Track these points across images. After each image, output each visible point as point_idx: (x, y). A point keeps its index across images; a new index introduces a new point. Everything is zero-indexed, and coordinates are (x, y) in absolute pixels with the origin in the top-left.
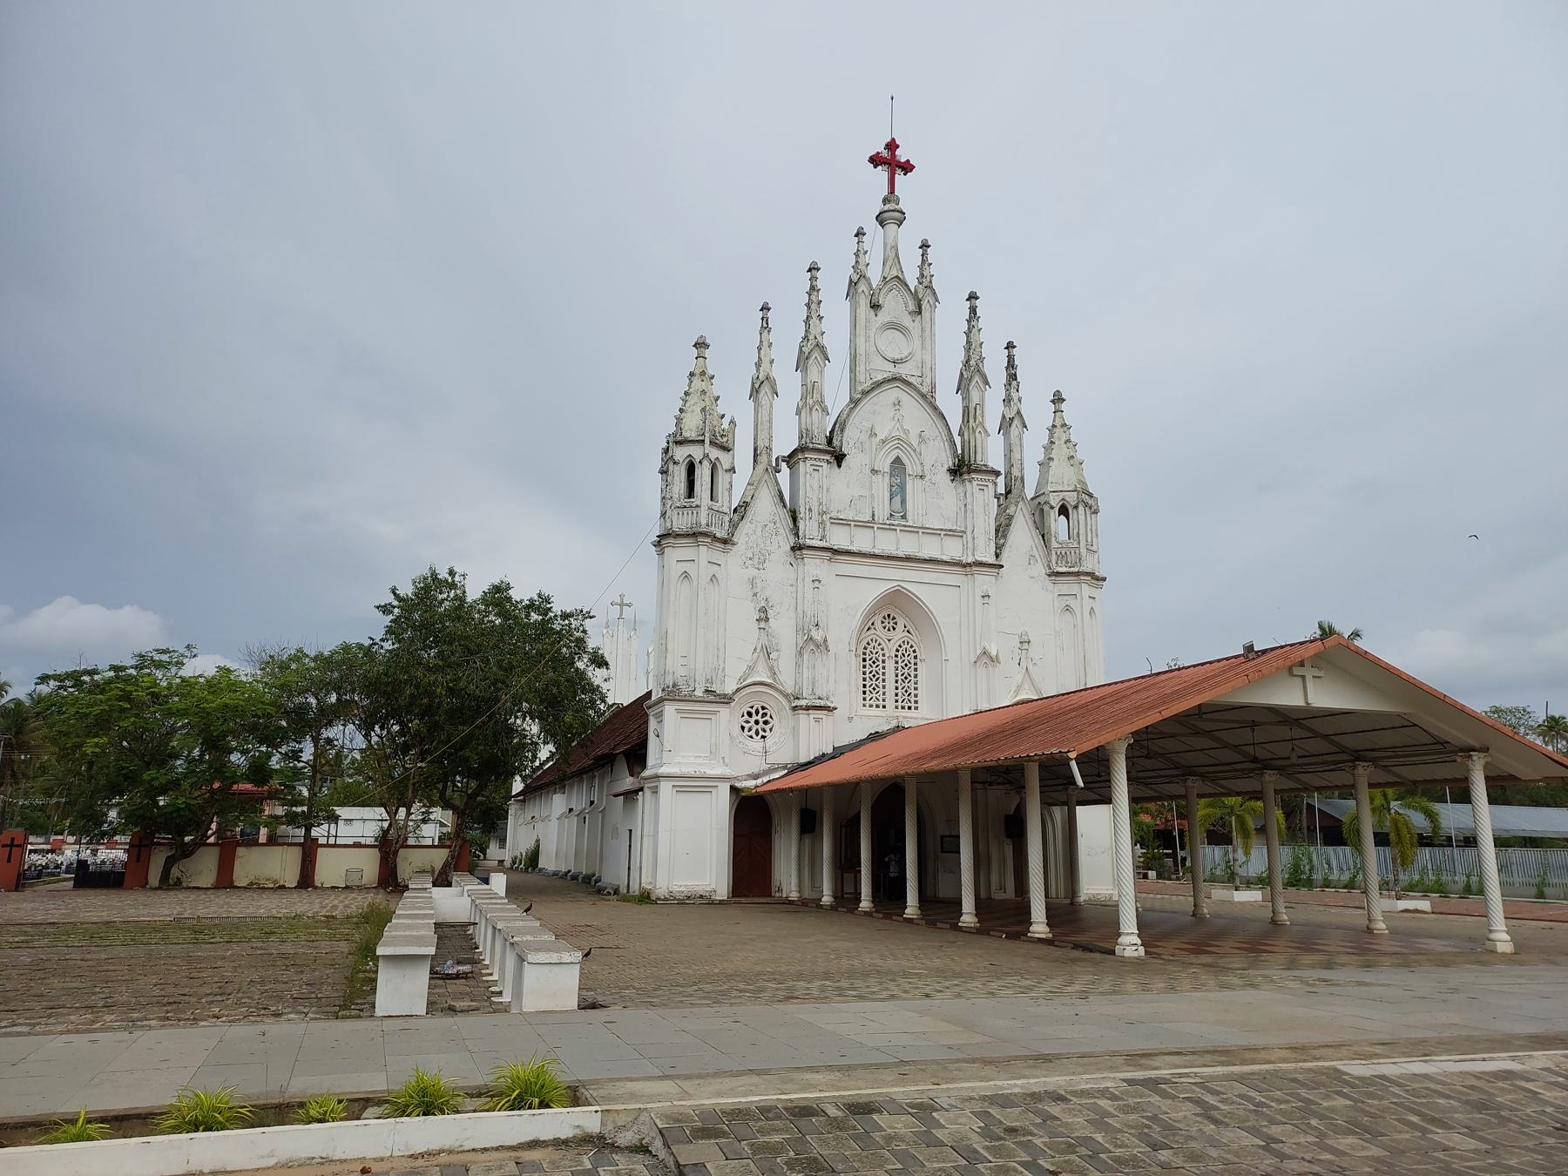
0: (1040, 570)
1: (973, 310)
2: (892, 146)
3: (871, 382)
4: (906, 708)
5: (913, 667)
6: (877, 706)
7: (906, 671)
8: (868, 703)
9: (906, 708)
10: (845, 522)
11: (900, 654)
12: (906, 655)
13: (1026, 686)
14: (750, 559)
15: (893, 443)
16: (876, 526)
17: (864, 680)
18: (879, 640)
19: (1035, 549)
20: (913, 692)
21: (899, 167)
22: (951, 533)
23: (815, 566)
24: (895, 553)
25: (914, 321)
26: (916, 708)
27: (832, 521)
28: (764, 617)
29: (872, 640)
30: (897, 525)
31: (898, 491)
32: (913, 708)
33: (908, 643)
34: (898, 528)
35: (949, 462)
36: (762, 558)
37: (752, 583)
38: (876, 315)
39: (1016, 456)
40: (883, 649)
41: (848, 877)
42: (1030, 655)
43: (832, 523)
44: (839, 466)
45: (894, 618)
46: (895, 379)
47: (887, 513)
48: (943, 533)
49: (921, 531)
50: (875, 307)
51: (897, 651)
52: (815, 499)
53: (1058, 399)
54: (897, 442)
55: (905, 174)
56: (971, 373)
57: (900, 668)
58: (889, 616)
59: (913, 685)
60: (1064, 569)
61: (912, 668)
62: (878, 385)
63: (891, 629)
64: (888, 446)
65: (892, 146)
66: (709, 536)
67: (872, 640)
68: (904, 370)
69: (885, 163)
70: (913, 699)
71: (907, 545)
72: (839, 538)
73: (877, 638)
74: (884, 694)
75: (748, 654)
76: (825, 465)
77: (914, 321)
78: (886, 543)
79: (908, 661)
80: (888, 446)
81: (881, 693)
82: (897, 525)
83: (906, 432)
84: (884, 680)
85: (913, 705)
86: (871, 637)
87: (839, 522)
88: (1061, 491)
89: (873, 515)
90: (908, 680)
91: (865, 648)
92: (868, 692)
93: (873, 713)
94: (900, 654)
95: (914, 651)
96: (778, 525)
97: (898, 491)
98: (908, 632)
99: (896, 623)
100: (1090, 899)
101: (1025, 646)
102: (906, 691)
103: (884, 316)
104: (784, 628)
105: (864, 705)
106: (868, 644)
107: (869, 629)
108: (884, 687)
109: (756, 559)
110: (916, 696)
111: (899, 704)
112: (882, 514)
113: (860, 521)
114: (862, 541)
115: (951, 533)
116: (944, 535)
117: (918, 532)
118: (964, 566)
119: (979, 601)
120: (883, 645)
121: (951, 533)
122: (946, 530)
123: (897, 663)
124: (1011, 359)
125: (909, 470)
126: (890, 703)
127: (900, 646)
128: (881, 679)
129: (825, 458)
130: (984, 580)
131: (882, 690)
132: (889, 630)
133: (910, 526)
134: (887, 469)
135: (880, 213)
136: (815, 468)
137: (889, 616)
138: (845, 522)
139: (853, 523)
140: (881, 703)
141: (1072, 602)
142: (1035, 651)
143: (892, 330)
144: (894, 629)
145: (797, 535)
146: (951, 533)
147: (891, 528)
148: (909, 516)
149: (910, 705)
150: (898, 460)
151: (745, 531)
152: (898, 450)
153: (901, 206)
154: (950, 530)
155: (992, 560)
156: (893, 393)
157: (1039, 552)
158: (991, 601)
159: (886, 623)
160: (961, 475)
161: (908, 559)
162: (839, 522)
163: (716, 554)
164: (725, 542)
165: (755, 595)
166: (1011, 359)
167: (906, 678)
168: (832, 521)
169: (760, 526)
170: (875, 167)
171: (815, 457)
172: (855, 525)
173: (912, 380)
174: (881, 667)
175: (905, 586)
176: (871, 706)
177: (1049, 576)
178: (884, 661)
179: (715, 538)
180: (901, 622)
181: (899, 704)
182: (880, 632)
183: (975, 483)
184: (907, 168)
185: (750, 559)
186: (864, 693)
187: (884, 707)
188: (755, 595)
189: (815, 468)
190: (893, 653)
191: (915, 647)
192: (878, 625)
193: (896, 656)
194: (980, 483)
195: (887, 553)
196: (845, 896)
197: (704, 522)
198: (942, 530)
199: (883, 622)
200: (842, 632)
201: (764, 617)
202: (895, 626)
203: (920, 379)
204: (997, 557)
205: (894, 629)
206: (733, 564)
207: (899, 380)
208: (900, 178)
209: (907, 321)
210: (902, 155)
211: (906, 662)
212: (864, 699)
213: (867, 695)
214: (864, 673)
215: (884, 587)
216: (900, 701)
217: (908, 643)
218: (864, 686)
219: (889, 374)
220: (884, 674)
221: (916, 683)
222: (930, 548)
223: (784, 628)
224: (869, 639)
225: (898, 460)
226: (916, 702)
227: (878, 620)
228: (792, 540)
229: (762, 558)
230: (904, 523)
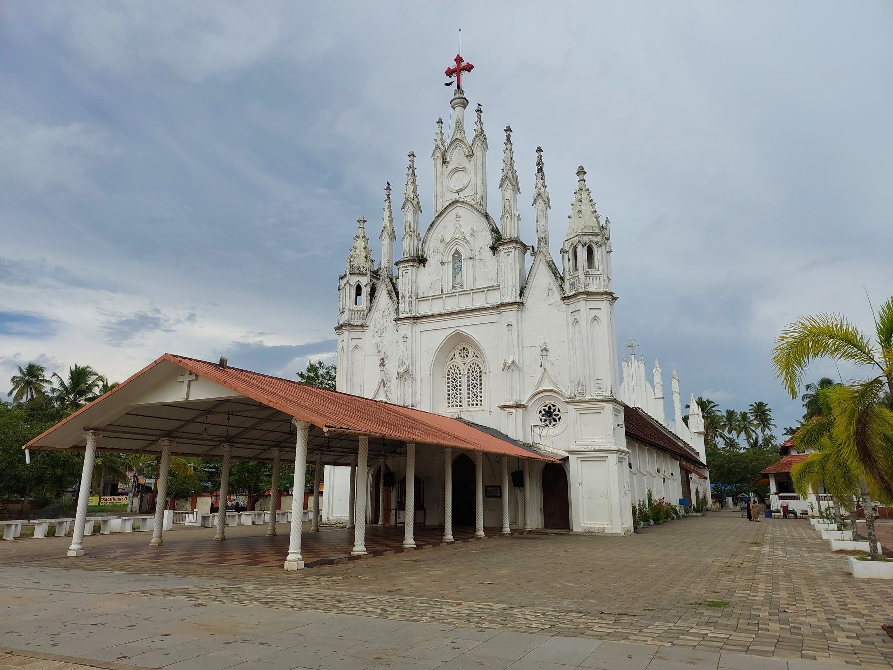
0: (557, 296)
1: (508, 138)
2: (459, 59)
3: (443, 209)
4: (475, 405)
5: (470, 379)
6: (457, 406)
7: (475, 382)
8: (451, 405)
9: (475, 405)
10: (426, 298)
11: (478, 371)
12: (474, 371)
13: (546, 381)
14: (376, 332)
15: (453, 242)
16: (444, 296)
17: (449, 391)
18: (458, 365)
19: (552, 284)
20: (479, 394)
21: (463, 70)
22: (491, 289)
23: (406, 329)
24: (454, 310)
25: (470, 161)
26: (481, 405)
27: (419, 300)
28: (382, 363)
29: (453, 366)
30: (456, 292)
31: (457, 270)
32: (479, 405)
33: (476, 363)
34: (457, 294)
35: (489, 241)
36: (382, 330)
37: (377, 345)
38: (447, 168)
39: (542, 223)
40: (460, 371)
41: (420, 513)
42: (549, 358)
43: (419, 301)
44: (424, 266)
45: (468, 350)
46: (454, 203)
47: (450, 286)
48: (486, 290)
49: (471, 292)
50: (444, 162)
51: (469, 369)
52: (407, 290)
53: (581, 172)
54: (456, 240)
55: (470, 72)
56: (510, 179)
57: (471, 380)
58: (464, 349)
59: (479, 390)
60: (573, 293)
61: (479, 380)
62: (446, 208)
63: (465, 356)
64: (450, 246)
65: (459, 59)
66: (348, 325)
67: (453, 366)
68: (462, 196)
69: (456, 72)
70: (479, 399)
71: (465, 303)
72: (424, 309)
73: (476, 362)
74: (461, 398)
75: (375, 387)
76: (410, 268)
77: (470, 161)
78: (452, 305)
79: (477, 376)
80: (450, 246)
81: (459, 398)
82: (456, 292)
83: (462, 233)
84: (461, 390)
85: (479, 403)
86: (472, 362)
87: (424, 299)
88: (570, 239)
89: (442, 290)
90: (476, 387)
91: (449, 371)
92: (451, 398)
93: (480, 409)
94: (470, 371)
95: (480, 368)
96: (390, 309)
97: (457, 270)
98: (477, 356)
99: (468, 353)
100: (585, 531)
101: (545, 353)
102: (475, 395)
103: (451, 166)
104: (393, 368)
105: (449, 407)
106: (451, 368)
107: (453, 359)
108: (461, 394)
109: (379, 332)
110: (481, 397)
111: (471, 403)
112: (447, 288)
113: (433, 296)
114: (438, 307)
115: (491, 289)
116: (487, 291)
117: (470, 293)
118: (498, 307)
119: (506, 328)
120: (460, 368)
121: (490, 289)
122: (487, 287)
123: (469, 377)
124: (540, 158)
125: (464, 257)
126: (465, 403)
127: (471, 367)
128: (459, 389)
129: (410, 264)
130: (510, 315)
131: (459, 396)
132: (464, 358)
133: (464, 291)
134: (450, 259)
135: (451, 103)
136: (406, 272)
137: (464, 349)
138: (426, 298)
139: (430, 298)
140: (459, 404)
141: (577, 315)
142: (551, 356)
143: (459, 172)
144: (467, 356)
145: (397, 311)
146: (490, 289)
147: (453, 295)
148: (465, 286)
149: (477, 403)
150: (457, 251)
151: (374, 317)
152: (457, 246)
153: (465, 96)
154: (490, 287)
155: (518, 300)
156: (459, 210)
157: (554, 284)
158: (514, 328)
159: (462, 354)
160: (496, 249)
161: (461, 312)
162: (424, 299)
163: (357, 333)
164: (362, 326)
165: (379, 352)
166: (540, 158)
167: (475, 386)
168: (419, 300)
169: (381, 312)
170: (451, 77)
171: (404, 265)
172: (432, 299)
173: (468, 199)
174: (459, 381)
175: (462, 330)
176: (453, 406)
177: (563, 300)
178: (460, 378)
179: (353, 326)
180: (471, 351)
181: (471, 403)
182: (459, 361)
183: (502, 252)
184: (469, 68)
185: (376, 332)
186: (449, 398)
187: (449, 407)
188: (379, 352)
189: (406, 272)
190: (467, 371)
191: (480, 366)
192: (457, 355)
193: (468, 373)
194: (506, 251)
195: (450, 311)
196: (397, 525)
197: (347, 318)
198: (485, 288)
199: (460, 354)
200: (424, 366)
201: (382, 363)
202: (468, 354)
203: (472, 197)
204: (521, 297)
205: (467, 356)
206: (368, 339)
207: (457, 202)
208: (465, 75)
209: (466, 163)
210: (463, 64)
211: (475, 376)
212: (449, 403)
213: (470, 399)
214: (449, 387)
215: (447, 333)
216: (457, 404)
217: (476, 363)
218: (449, 395)
219: (453, 201)
220: (461, 386)
221: (481, 389)
222: (480, 301)
223: (393, 368)
224: (451, 365)
225: (457, 251)
226: (481, 401)
227: (457, 352)
228: (395, 316)
229: (382, 330)
230: (460, 290)
